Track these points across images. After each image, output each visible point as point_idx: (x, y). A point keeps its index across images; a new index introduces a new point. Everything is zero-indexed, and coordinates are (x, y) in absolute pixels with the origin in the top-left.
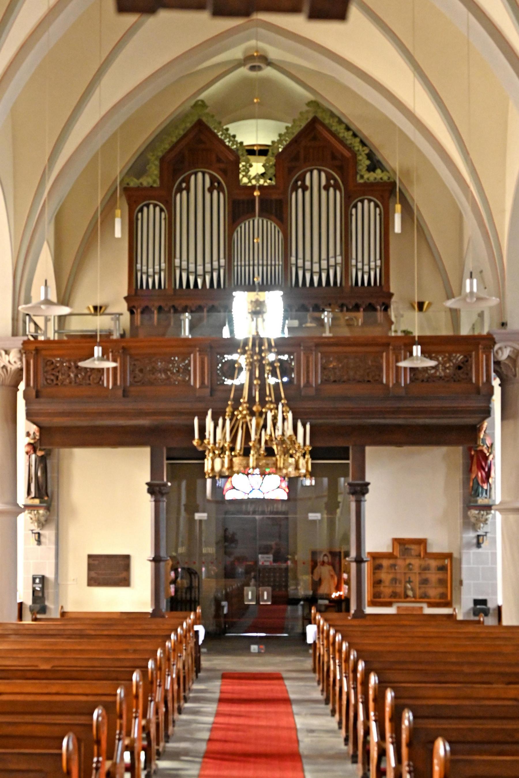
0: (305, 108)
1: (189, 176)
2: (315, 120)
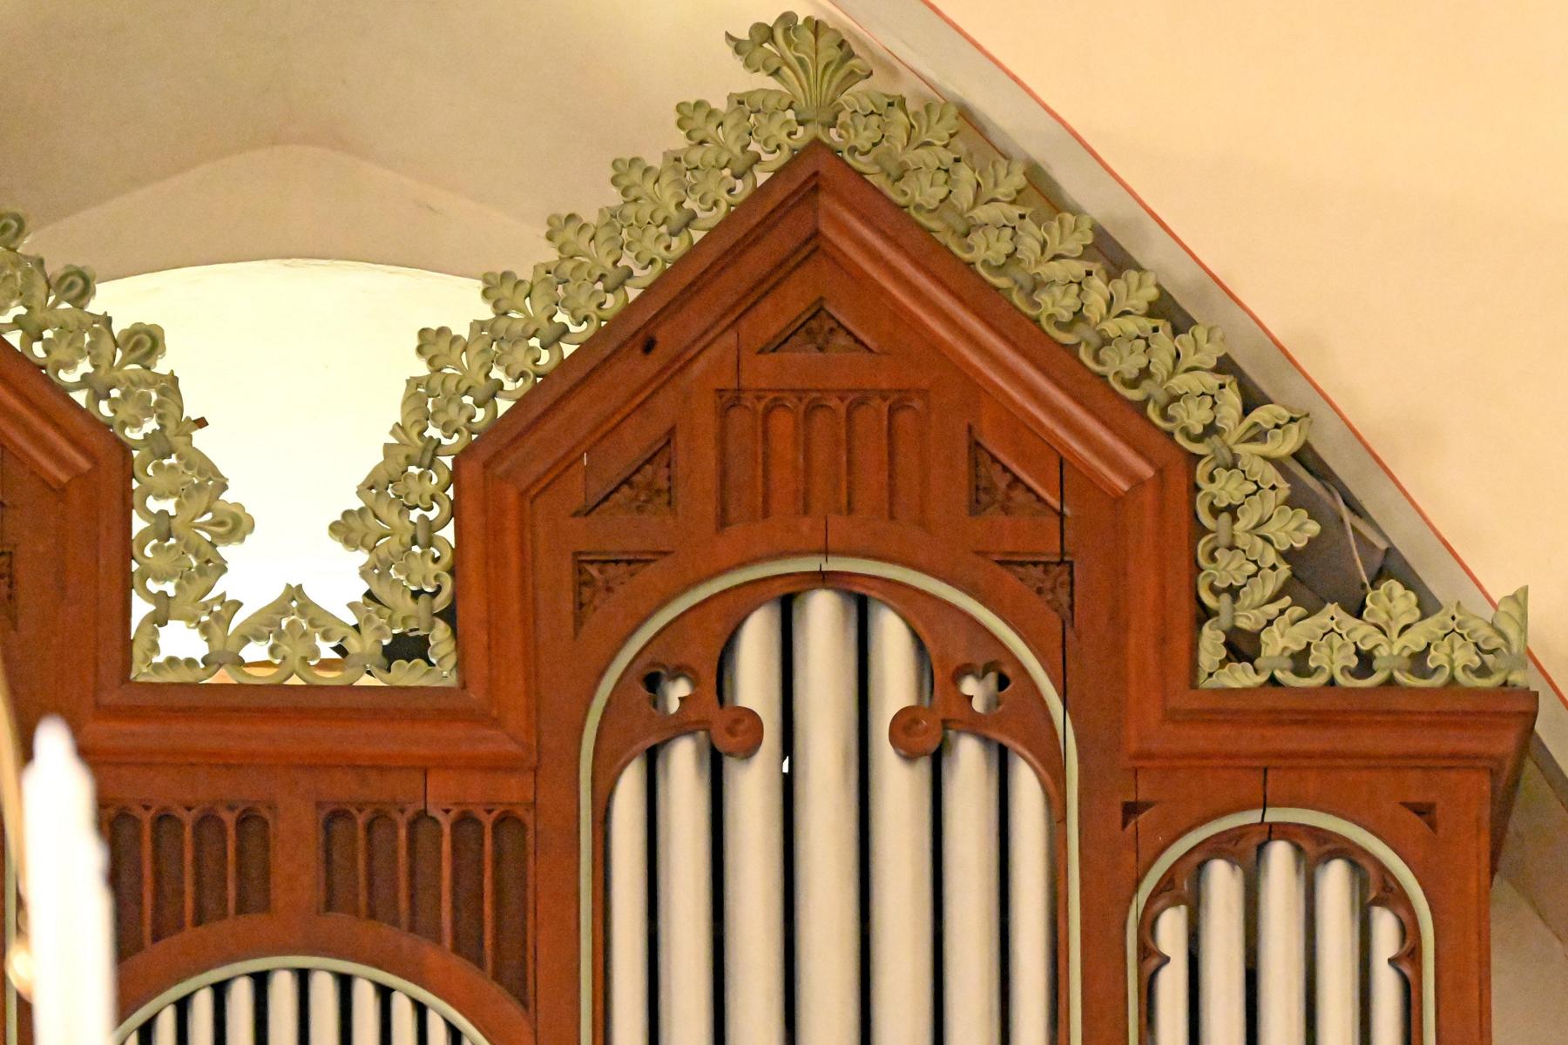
2: (814, 179)
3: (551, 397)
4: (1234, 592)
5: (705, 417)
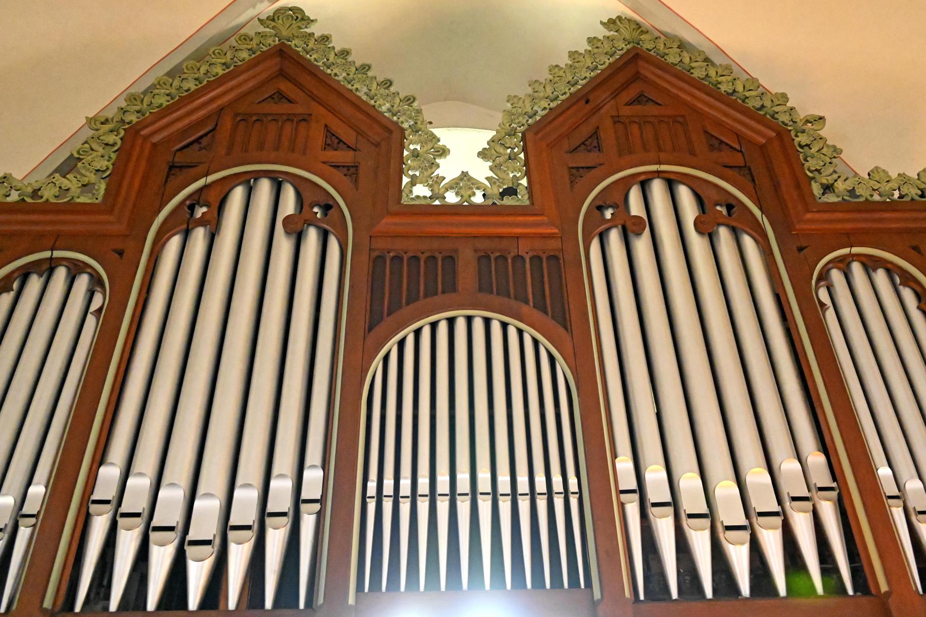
0: (601, 32)
1: (228, 184)
3: (553, 116)
4: (818, 171)
5: (608, 122)
